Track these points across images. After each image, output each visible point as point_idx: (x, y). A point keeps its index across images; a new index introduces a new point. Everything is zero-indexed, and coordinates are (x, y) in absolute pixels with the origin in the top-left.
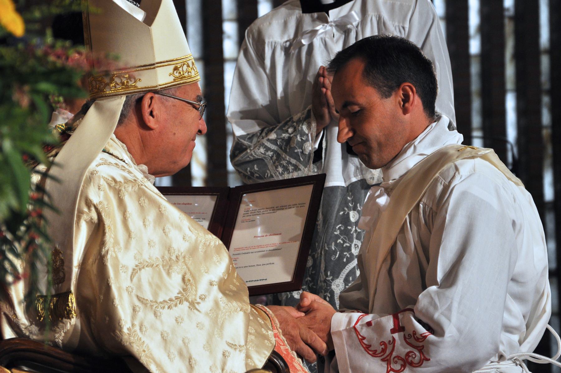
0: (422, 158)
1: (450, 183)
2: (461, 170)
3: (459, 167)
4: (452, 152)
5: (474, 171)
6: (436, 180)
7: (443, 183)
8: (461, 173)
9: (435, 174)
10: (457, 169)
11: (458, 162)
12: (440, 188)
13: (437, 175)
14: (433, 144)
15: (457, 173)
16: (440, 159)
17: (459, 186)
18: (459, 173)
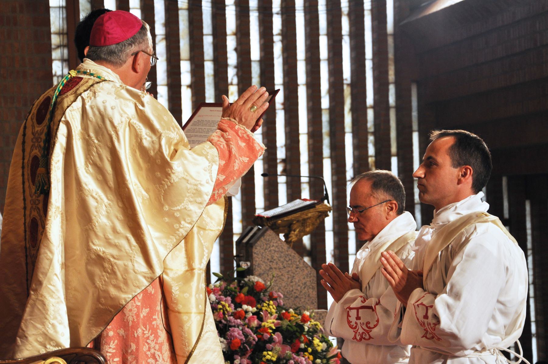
0: (459, 216)
1: (470, 236)
2: (478, 229)
4: (474, 216)
6: (462, 233)
9: (461, 229)
10: (475, 228)
11: (477, 225)
12: (464, 239)
13: (463, 230)
14: (468, 208)
16: (466, 221)
17: (474, 239)
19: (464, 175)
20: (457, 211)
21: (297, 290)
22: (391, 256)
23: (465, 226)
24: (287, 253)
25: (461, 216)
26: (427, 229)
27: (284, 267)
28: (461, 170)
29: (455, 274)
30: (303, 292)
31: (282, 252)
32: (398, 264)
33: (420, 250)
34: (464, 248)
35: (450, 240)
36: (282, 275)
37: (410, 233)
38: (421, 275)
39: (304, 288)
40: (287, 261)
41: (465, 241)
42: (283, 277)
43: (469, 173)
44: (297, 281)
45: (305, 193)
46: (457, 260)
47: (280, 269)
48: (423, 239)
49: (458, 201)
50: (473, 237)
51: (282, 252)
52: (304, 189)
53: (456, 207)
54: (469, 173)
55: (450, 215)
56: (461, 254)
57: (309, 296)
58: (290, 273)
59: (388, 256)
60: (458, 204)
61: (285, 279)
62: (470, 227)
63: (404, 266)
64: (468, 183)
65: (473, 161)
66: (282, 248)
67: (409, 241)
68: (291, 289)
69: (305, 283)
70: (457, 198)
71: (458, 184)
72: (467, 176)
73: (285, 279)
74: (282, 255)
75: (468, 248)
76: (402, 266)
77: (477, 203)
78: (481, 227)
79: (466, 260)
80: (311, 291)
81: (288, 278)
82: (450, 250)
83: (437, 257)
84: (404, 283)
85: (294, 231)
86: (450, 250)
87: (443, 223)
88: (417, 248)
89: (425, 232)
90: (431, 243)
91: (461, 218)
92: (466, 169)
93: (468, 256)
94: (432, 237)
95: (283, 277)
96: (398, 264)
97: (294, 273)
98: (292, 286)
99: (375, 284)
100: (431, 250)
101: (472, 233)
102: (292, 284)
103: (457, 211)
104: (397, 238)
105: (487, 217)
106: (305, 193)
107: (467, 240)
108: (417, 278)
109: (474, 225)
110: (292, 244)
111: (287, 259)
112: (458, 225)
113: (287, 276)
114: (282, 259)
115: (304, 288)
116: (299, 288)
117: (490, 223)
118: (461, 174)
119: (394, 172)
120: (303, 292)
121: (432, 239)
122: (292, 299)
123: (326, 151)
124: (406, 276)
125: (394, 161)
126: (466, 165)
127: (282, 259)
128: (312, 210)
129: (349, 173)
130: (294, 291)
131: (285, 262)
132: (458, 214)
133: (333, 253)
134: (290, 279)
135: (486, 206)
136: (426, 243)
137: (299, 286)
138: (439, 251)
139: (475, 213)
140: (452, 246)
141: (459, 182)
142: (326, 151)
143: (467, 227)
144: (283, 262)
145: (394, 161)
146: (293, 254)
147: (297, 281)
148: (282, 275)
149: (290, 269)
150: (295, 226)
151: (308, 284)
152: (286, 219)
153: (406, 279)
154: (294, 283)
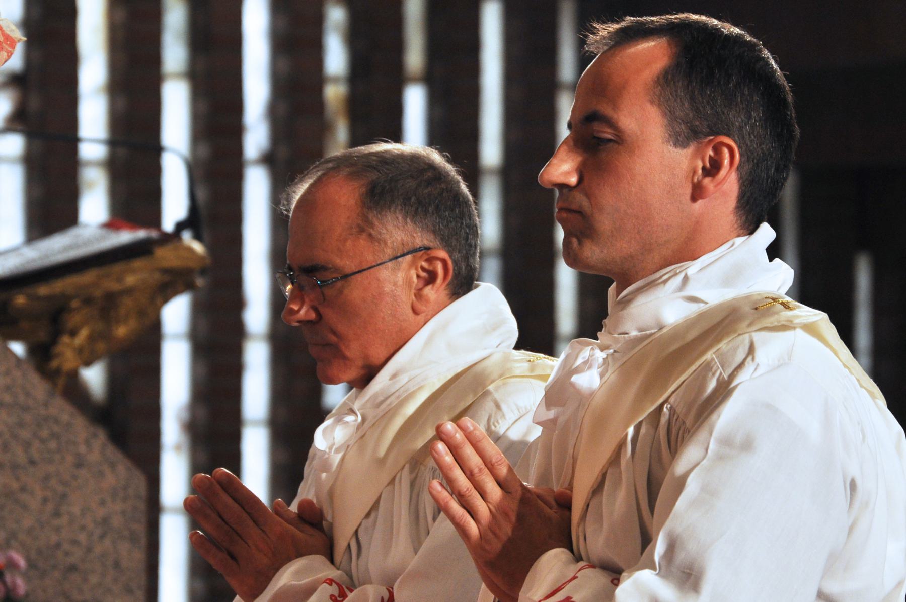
0: (694, 309)
1: (732, 376)
2: (760, 354)
3: (756, 345)
4: (747, 309)
5: (790, 359)
6: (708, 367)
7: (718, 374)
8: (757, 360)
9: (704, 352)
10: (751, 350)
11: (758, 337)
12: (712, 385)
13: (709, 355)
14: (728, 281)
15: (750, 358)
16: (723, 323)
18: (753, 359)
19: (713, 169)
20: (690, 291)
21: (75, 542)
22: (469, 436)
23: (718, 340)
24: (43, 412)
25: (701, 307)
26: (586, 353)
27: (32, 462)
28: (699, 153)
29: (681, 503)
30: (98, 550)
31: (26, 409)
32: (490, 466)
33: (561, 420)
34: (714, 417)
35: (665, 388)
36: (23, 489)
37: (497, 358)
38: (564, 503)
39: (102, 537)
40: (43, 441)
41: (716, 391)
42: (24, 497)
43: (726, 161)
44: (76, 510)
45: (94, 206)
46: (689, 455)
47: (15, 467)
48: (573, 385)
49: (694, 258)
50: (743, 377)
51: (26, 409)
52: (91, 185)
53: (686, 279)
54: (726, 161)
55: (664, 306)
56: (702, 435)
57: (117, 565)
58: (53, 482)
59: (459, 436)
60: (693, 268)
61: (34, 503)
62: (732, 347)
63: (510, 470)
64: (724, 194)
65: (737, 118)
66: (28, 394)
67: (491, 387)
68: (54, 538)
69: (105, 521)
70: (687, 250)
71: (694, 199)
72: (723, 172)
73: (34, 503)
74: (27, 418)
75: (726, 416)
76: (503, 471)
77: (749, 267)
78: (771, 347)
79: (720, 458)
80: (124, 547)
81: (45, 500)
82: (664, 420)
83: (621, 445)
84: (507, 529)
85: (73, 333)
86: (664, 420)
87: (640, 330)
88: (551, 414)
89: (579, 361)
90: (598, 400)
91: (701, 316)
92: (717, 149)
93: (726, 442)
94: (602, 376)
95: (24, 497)
96: (490, 466)
97: (65, 484)
98: (58, 529)
99: (378, 535)
100: (601, 420)
101: (741, 366)
102: (56, 522)
103: (690, 291)
104: (450, 376)
105: (789, 313)
106: (94, 206)
107: (724, 390)
108: (552, 513)
109: (746, 339)
110: (61, 381)
111: (45, 433)
112: (691, 336)
113: (39, 494)
114: (25, 434)
115: (102, 537)
116: (82, 537)
117: (799, 332)
118: (700, 164)
119: (414, 138)
120: (98, 550)
121: (601, 387)
122: (57, 574)
123: (174, 53)
124: (513, 506)
125: (415, 102)
126: (717, 134)
127: (25, 434)
128: (138, 263)
129: (256, 137)
130: (66, 546)
131: (36, 444)
132: (693, 299)
133: (185, 415)
134: (50, 507)
135: (781, 276)
136: (583, 398)
137: (83, 528)
138: (627, 426)
139: (748, 297)
140: (672, 410)
141: (697, 192)
142: (174, 53)
143: (723, 345)
144: (27, 445)
145: (415, 102)
146: (65, 417)
147: (76, 510)
148: (23, 489)
149: (51, 469)
150: (74, 319)
151: (116, 522)
152: (43, 290)
153: (514, 519)
154: (64, 520)
